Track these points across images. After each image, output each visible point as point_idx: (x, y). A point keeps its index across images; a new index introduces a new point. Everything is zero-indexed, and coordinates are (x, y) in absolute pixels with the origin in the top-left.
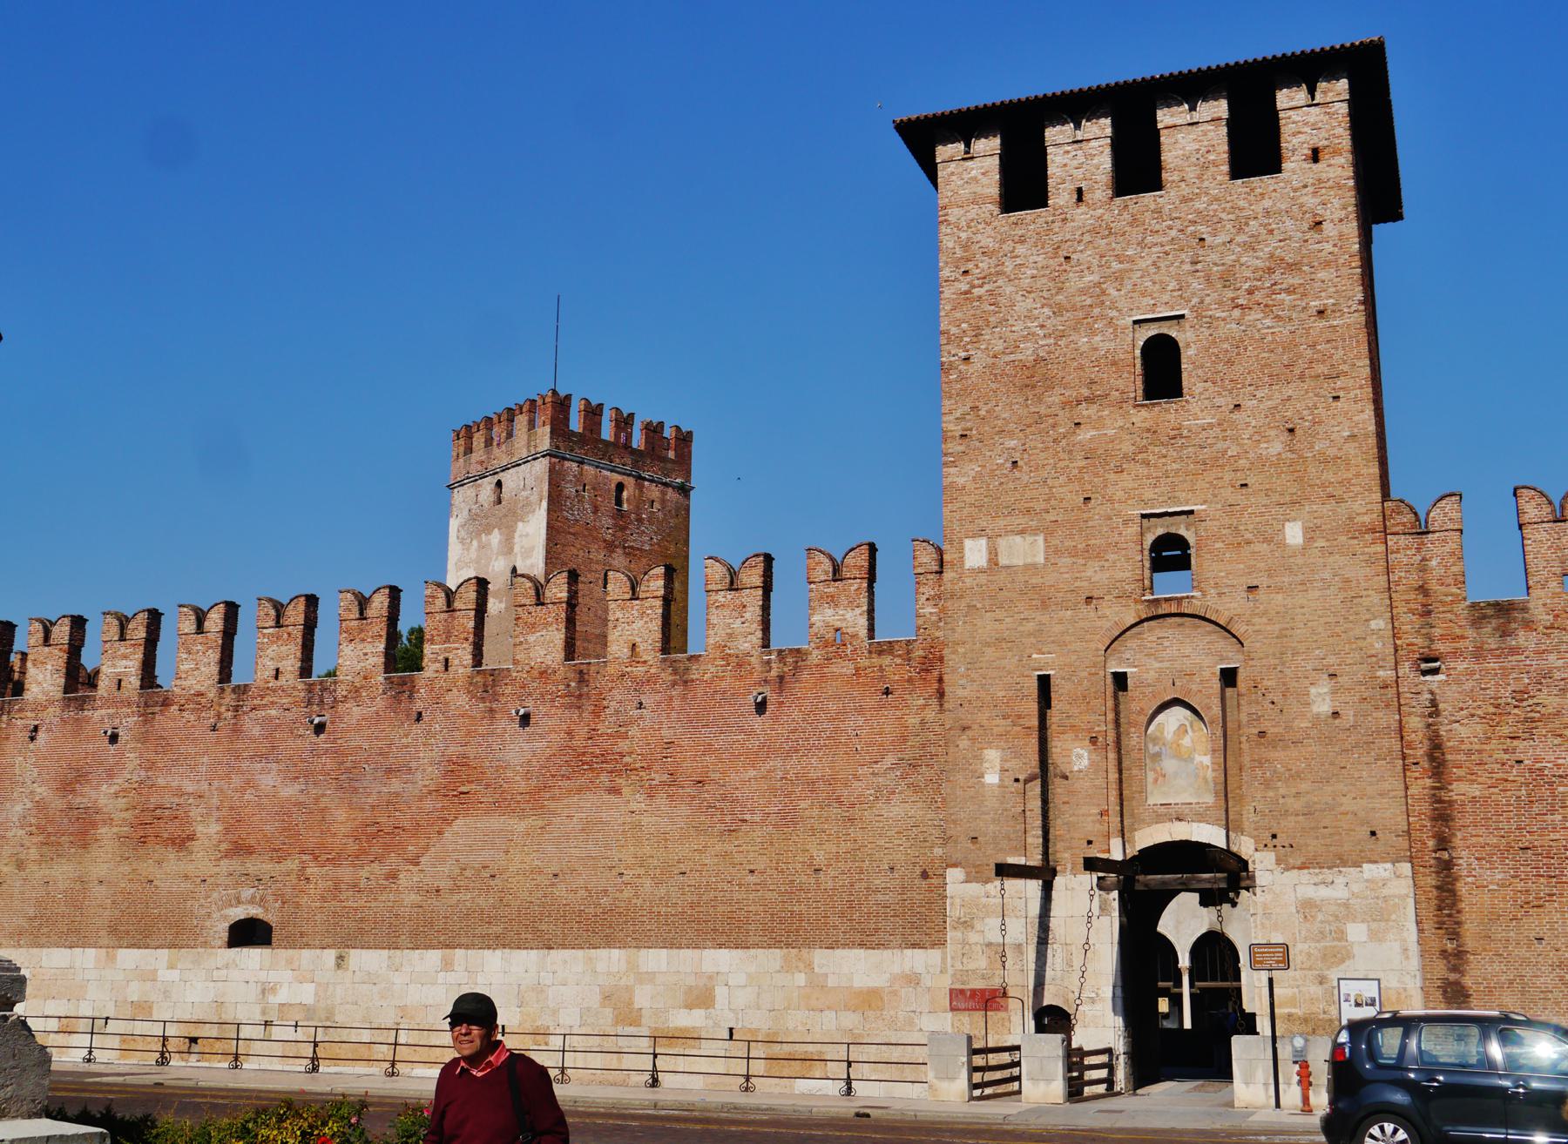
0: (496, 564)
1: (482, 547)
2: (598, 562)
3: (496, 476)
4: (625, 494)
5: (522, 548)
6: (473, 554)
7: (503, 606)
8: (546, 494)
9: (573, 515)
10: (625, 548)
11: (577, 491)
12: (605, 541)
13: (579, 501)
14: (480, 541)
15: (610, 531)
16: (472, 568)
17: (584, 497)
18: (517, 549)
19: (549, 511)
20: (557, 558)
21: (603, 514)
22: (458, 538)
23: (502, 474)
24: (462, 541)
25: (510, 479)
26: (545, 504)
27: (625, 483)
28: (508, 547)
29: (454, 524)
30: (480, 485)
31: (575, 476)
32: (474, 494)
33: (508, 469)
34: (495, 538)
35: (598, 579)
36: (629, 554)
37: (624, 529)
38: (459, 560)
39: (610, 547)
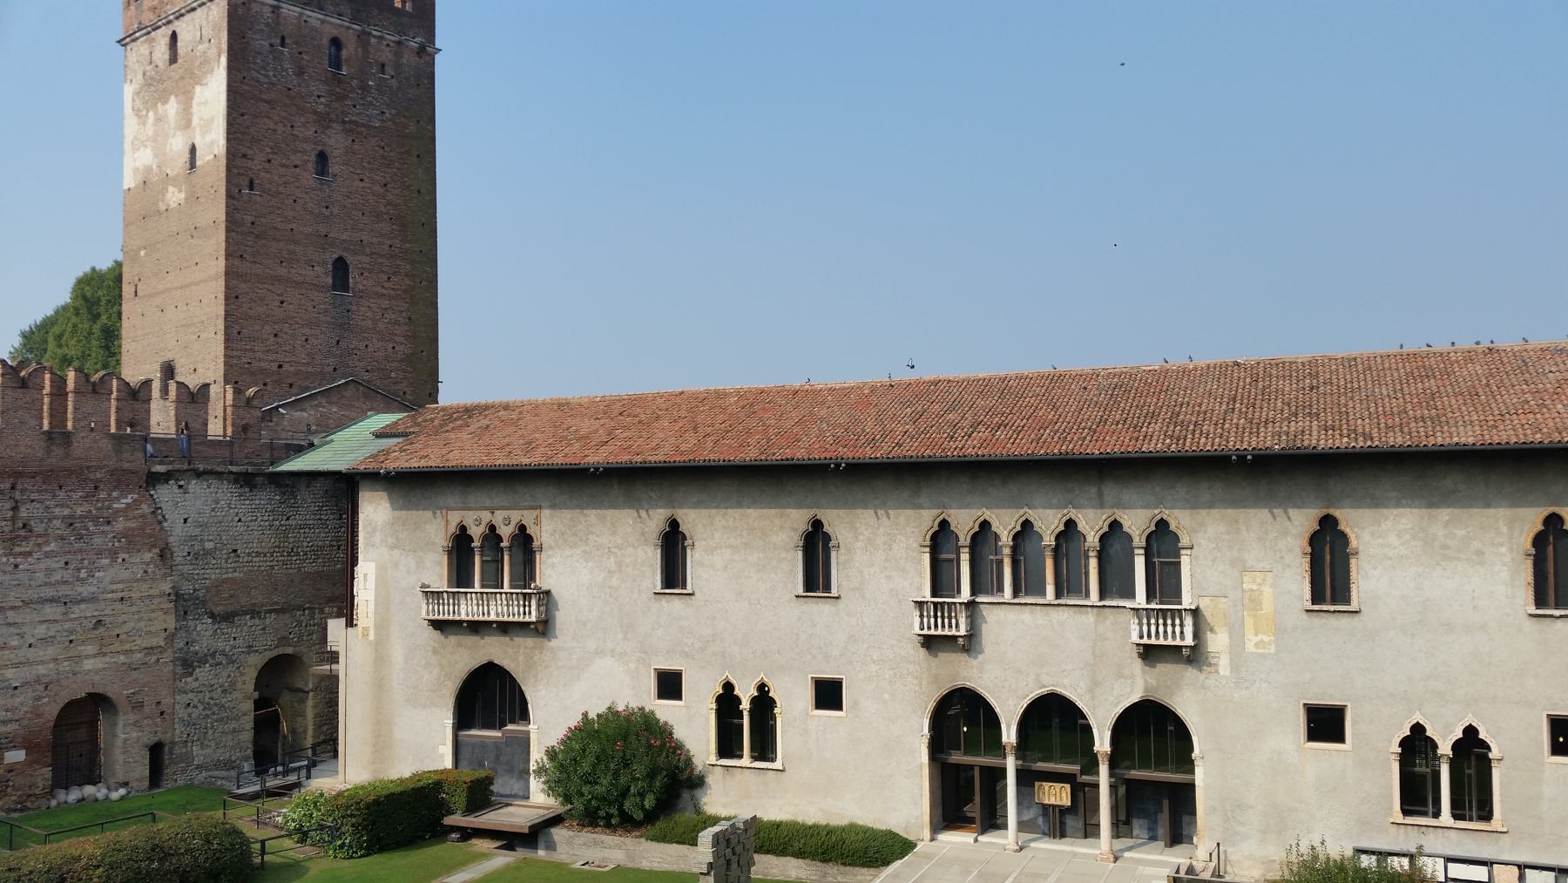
0: (173, 141)
1: (159, 120)
2: (305, 140)
3: (170, 26)
4: (344, 53)
5: (201, 119)
6: (150, 130)
7: (182, 196)
8: (225, 46)
9: (266, 76)
10: (344, 122)
11: (271, 45)
12: (315, 113)
13: (275, 58)
14: (156, 113)
15: (322, 100)
16: (150, 147)
17: (282, 53)
18: (195, 121)
19: (231, 69)
20: (243, 133)
21: (310, 76)
22: (133, 110)
23: (176, 23)
24: (137, 112)
25: (187, 29)
26: (224, 60)
27: (343, 39)
28: (186, 122)
29: (129, 91)
30: (153, 40)
31: (268, 25)
32: (147, 52)
33: (182, 15)
34: (172, 108)
35: (306, 162)
36: (351, 131)
37: (341, 98)
38: (135, 138)
39: (324, 120)
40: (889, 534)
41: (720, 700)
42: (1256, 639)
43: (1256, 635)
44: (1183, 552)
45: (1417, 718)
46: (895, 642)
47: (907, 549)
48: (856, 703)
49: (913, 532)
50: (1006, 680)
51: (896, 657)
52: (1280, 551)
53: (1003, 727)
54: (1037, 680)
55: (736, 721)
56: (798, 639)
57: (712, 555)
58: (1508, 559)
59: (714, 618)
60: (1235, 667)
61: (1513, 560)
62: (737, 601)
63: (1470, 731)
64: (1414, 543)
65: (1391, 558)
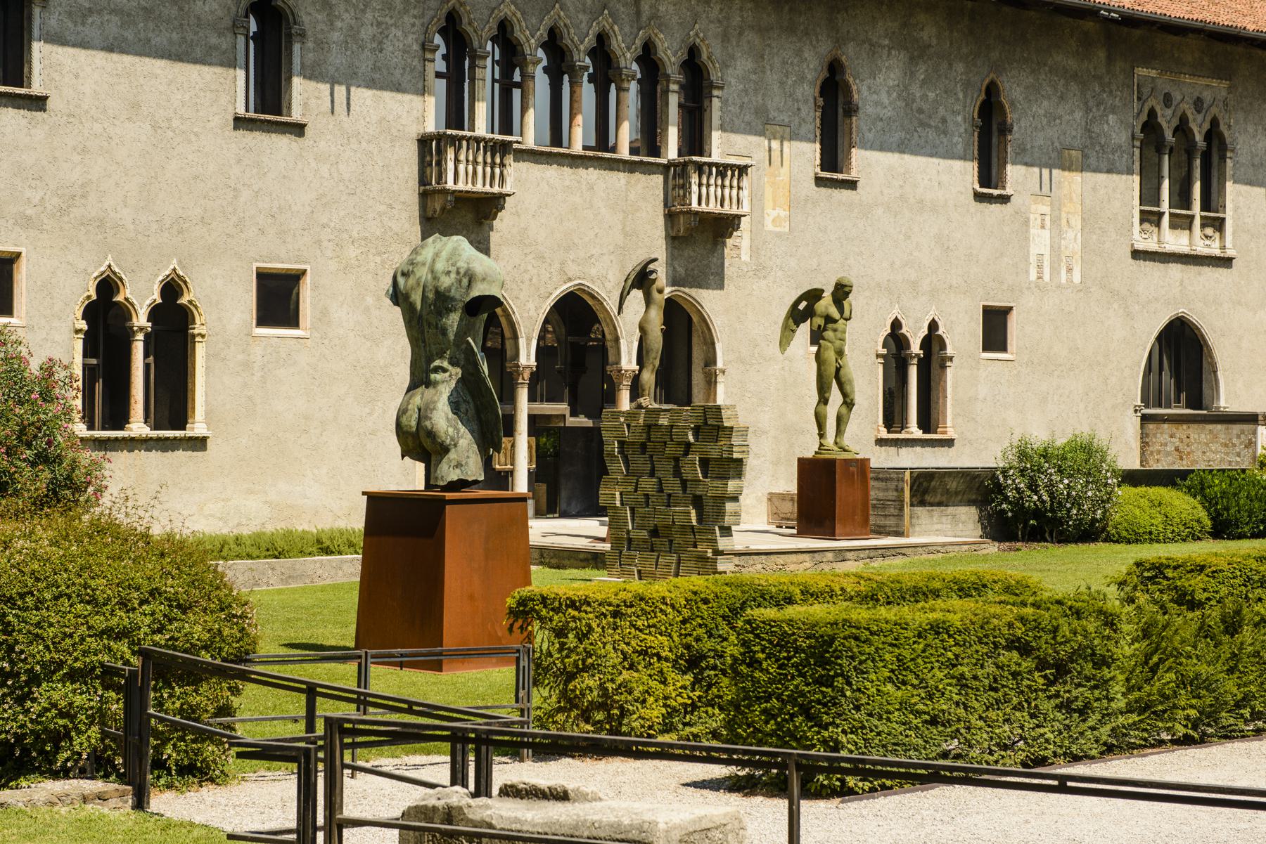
40: (379, 24)
41: (91, 312)
42: (774, 214)
43: (774, 209)
44: (715, 92)
45: (895, 313)
46: (382, 208)
47: (405, 52)
48: (323, 315)
49: (413, 25)
50: (526, 271)
51: (385, 232)
52: (798, 101)
53: (522, 342)
54: (562, 271)
55: (94, 361)
56: (235, 197)
57: (83, 24)
58: (962, 130)
59: (85, 150)
60: (754, 250)
61: (966, 130)
62: (129, 119)
63: (933, 326)
64: (898, 103)
65: (881, 120)
